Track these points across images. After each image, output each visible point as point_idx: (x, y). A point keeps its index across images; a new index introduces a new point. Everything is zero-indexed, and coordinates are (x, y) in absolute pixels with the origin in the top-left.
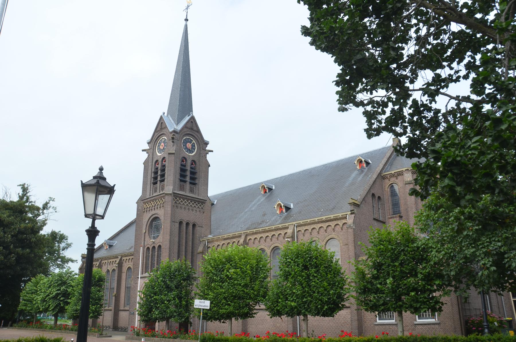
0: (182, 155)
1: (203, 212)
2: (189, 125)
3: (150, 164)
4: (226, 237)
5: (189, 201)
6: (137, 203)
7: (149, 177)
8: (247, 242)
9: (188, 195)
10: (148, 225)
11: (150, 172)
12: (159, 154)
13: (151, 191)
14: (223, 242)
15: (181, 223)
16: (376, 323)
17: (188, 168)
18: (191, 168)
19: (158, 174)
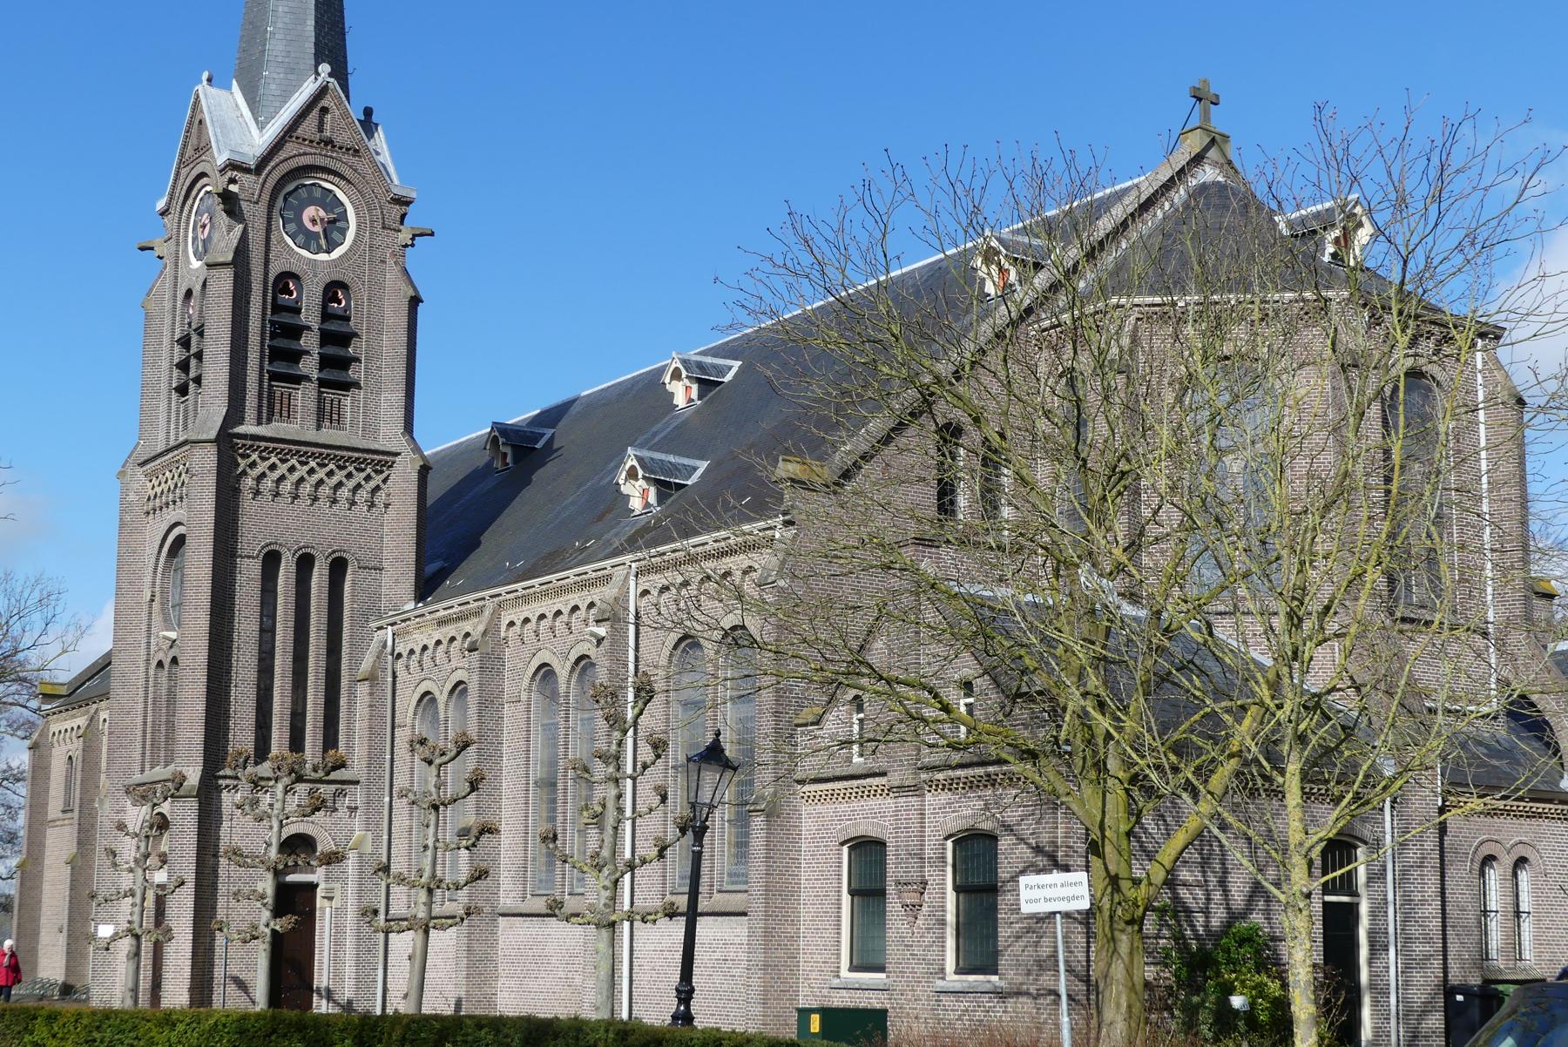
0: (274, 270)
1: (387, 506)
2: (308, 127)
3: (168, 305)
4: (442, 613)
5: (313, 464)
6: (122, 474)
7: (165, 364)
8: (503, 634)
9: (311, 435)
10: (160, 570)
11: (166, 341)
12: (196, 264)
13: (173, 426)
15: (271, 560)
16: (836, 982)
17: (310, 316)
18: (326, 316)
19: (192, 352)
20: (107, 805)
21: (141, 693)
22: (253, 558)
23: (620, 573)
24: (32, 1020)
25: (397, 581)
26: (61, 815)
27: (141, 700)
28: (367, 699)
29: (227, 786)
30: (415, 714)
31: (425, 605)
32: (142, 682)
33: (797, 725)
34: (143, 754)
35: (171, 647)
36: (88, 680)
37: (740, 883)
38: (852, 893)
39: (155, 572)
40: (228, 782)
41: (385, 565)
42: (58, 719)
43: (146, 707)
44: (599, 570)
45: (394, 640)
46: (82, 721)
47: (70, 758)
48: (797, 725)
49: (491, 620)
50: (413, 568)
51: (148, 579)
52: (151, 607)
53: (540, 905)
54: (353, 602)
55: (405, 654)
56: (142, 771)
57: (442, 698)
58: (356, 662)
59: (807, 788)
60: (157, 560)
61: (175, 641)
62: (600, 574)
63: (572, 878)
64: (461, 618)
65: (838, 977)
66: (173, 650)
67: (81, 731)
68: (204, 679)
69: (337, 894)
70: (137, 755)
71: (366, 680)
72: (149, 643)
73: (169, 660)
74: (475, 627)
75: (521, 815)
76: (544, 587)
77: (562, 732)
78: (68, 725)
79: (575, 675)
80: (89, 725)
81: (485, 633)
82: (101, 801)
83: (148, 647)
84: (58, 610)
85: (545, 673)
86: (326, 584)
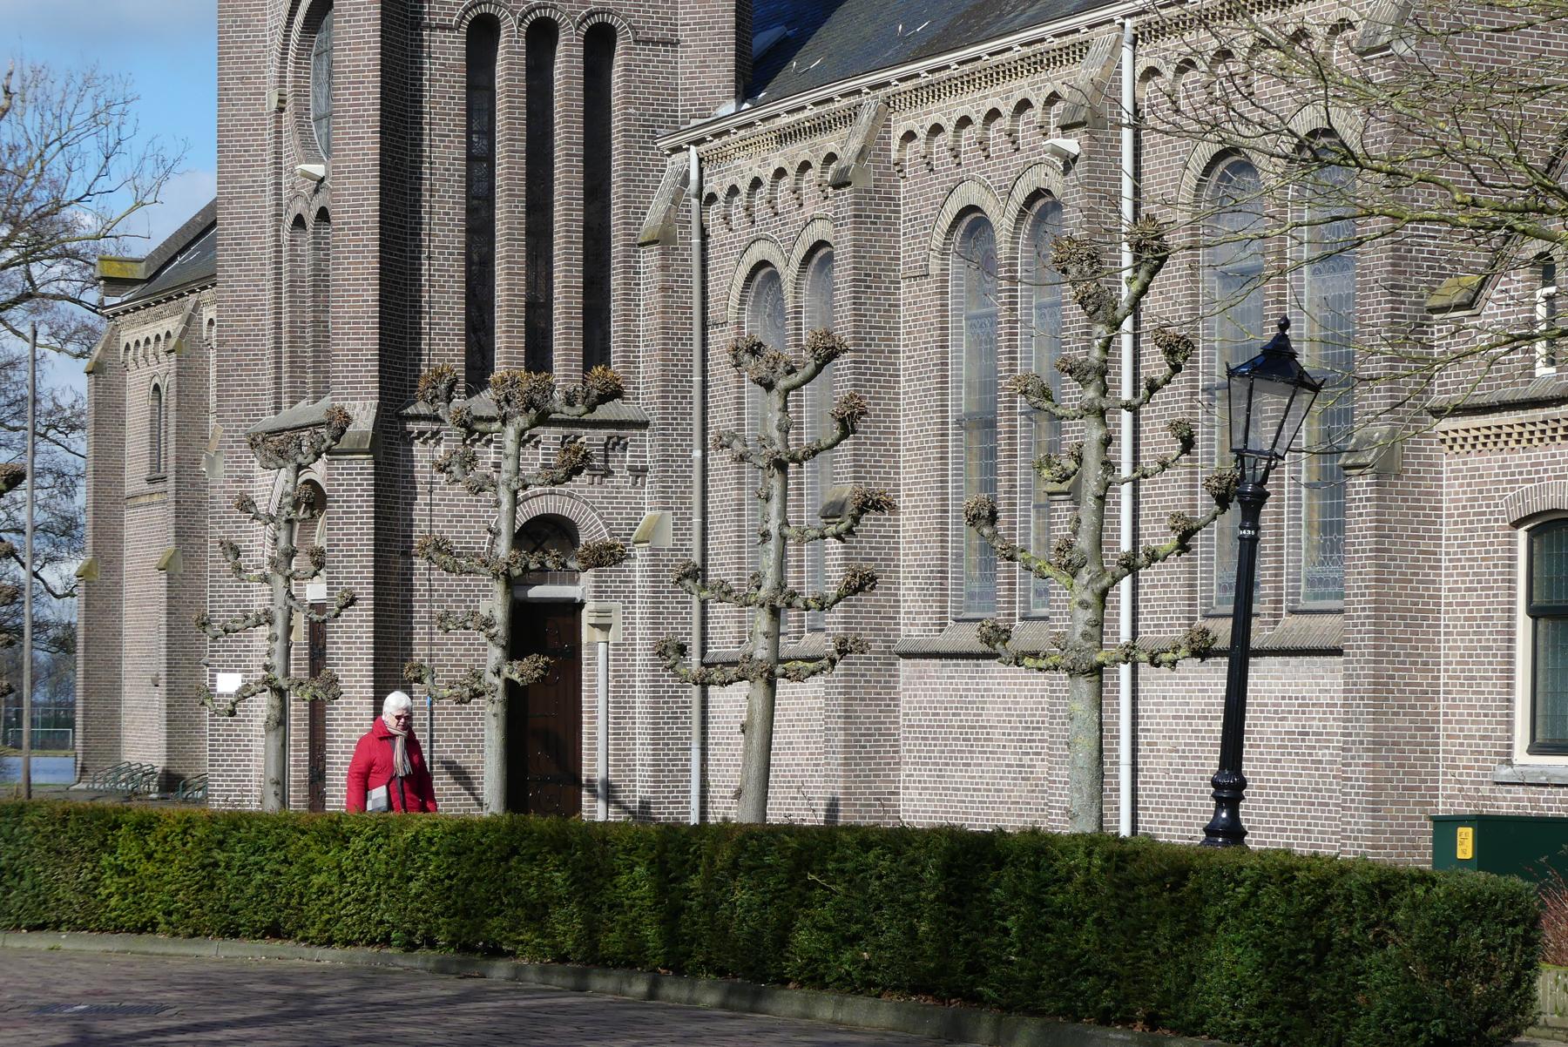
8: (894, 156)
10: (291, 55)
14: (777, 161)
16: (1504, 773)
20: (221, 469)
21: (270, 273)
22: (451, 29)
23: (1104, 35)
24: (112, 829)
25: (704, 65)
26: (146, 487)
27: (270, 285)
28: (658, 276)
29: (421, 433)
30: (742, 302)
31: (755, 107)
32: (269, 253)
33: (1433, 310)
34: (278, 378)
35: (316, 191)
36: (181, 252)
37: (1330, 596)
38: (1534, 612)
39: (283, 59)
40: (423, 425)
41: (682, 35)
42: (133, 322)
43: (278, 298)
44: (1066, 34)
45: (701, 170)
46: (173, 324)
47: (157, 388)
48: (1433, 310)
49: (873, 129)
50: (731, 39)
51: (272, 72)
52: (279, 121)
53: (968, 638)
54: (627, 103)
55: (721, 196)
56: (277, 409)
57: (788, 273)
58: (636, 211)
59: (1447, 424)
60: (287, 37)
61: (322, 180)
62: (1067, 40)
63: (1028, 590)
64: (820, 127)
65: (1509, 763)
66: (320, 196)
67: (172, 342)
68: (375, 246)
69: (617, 620)
70: (267, 381)
71: (655, 242)
72: (278, 185)
73: (314, 213)
74: (844, 143)
75: (933, 480)
76: (967, 68)
77: (1003, 329)
78: (150, 331)
79: (1026, 227)
80: (185, 331)
81: (861, 155)
82: (211, 463)
83: (278, 193)
84: (126, 131)
85: (972, 221)
86: (578, 73)
